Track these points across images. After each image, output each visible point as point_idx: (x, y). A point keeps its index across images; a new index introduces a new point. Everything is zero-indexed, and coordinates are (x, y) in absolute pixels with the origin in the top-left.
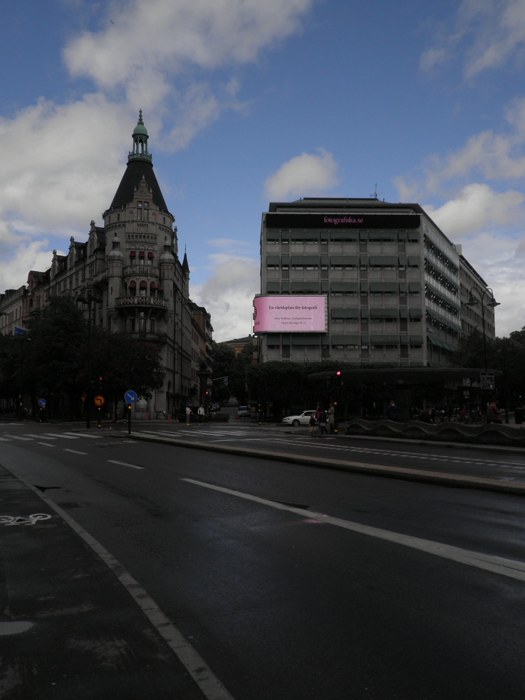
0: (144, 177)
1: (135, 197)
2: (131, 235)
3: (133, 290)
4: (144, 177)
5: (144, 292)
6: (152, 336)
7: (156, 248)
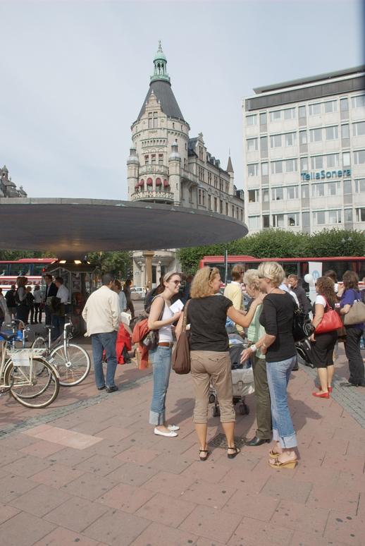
3: (142, 186)
5: (150, 188)
7: (165, 149)
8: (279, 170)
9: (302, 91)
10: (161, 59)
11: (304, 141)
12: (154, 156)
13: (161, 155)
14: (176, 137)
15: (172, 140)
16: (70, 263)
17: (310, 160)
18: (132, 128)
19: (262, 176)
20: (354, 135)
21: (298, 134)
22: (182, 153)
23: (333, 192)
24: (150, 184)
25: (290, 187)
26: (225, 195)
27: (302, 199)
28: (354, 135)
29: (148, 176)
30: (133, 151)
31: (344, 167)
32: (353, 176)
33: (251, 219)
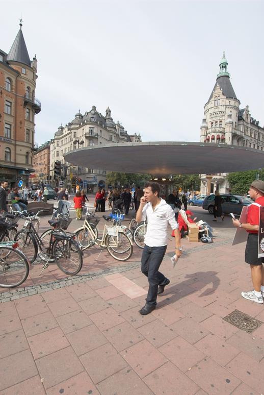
7: (224, 118)
12: (216, 122)
14: (231, 109)
15: (228, 112)
16: (160, 180)
22: (234, 119)
24: (213, 139)
29: (212, 134)
30: (204, 120)
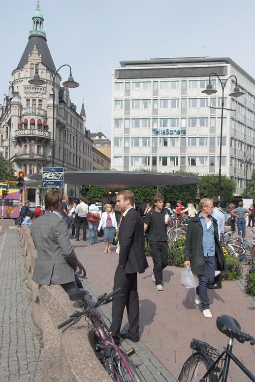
0: (35, 47)
1: (29, 60)
2: (26, 87)
3: (26, 125)
4: (35, 47)
5: (33, 126)
6: (38, 157)
7: (44, 96)
8: (137, 125)
9: (157, 71)
10: (39, 18)
11: (156, 107)
12: (34, 100)
13: (40, 101)
17: (159, 120)
18: (13, 74)
19: (125, 128)
20: (190, 107)
21: (152, 101)
23: (173, 145)
24: (33, 124)
25: (144, 139)
26: (80, 135)
27: (153, 147)
28: (190, 107)
29: (32, 117)
31: (181, 128)
32: (187, 135)
33: (115, 159)
